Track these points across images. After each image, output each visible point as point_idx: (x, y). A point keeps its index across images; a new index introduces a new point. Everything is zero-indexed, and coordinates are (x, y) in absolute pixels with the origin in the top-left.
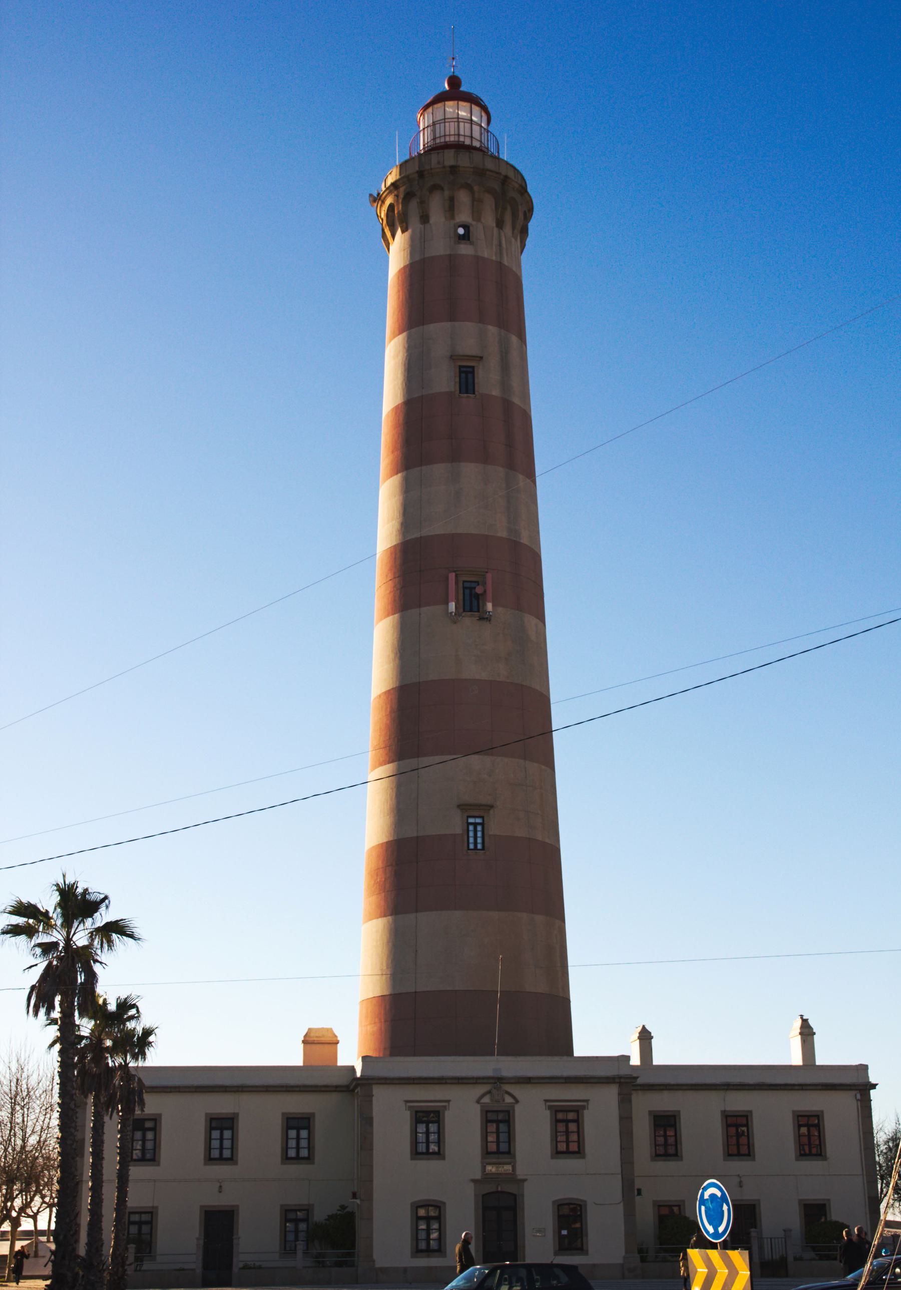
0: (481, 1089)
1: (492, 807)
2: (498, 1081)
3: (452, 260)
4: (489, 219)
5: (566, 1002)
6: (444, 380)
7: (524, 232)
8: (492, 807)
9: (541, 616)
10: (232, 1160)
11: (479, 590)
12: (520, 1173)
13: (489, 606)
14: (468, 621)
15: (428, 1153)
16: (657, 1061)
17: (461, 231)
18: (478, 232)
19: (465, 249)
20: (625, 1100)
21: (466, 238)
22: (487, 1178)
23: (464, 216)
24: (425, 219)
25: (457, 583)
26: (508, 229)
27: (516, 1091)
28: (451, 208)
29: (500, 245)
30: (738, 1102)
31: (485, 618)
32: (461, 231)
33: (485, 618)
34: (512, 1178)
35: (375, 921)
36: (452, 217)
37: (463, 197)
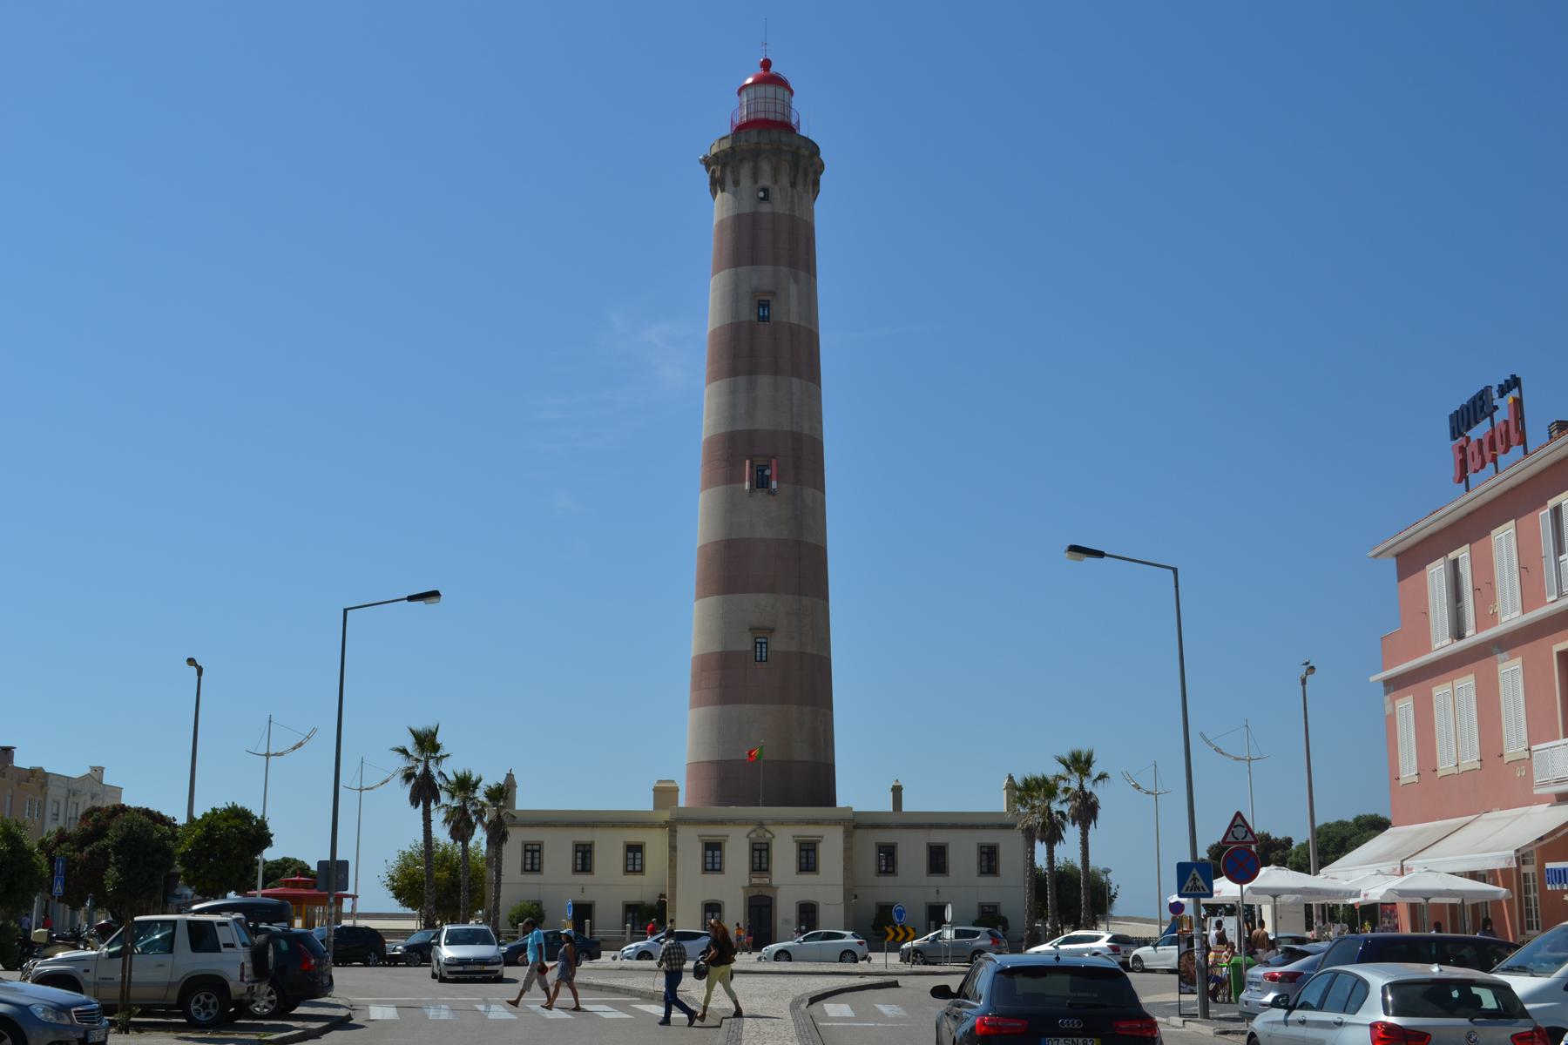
0: (750, 828)
1: (772, 630)
2: (761, 824)
3: (755, 217)
4: (785, 181)
5: (833, 767)
6: (747, 313)
7: (816, 183)
8: (772, 630)
9: (820, 487)
10: (539, 871)
11: (767, 472)
12: (774, 883)
13: (774, 485)
14: (760, 494)
15: (713, 870)
16: (905, 808)
17: (762, 194)
18: (776, 194)
19: (765, 208)
20: (848, 836)
21: (766, 199)
22: (752, 886)
23: (765, 181)
24: (736, 183)
25: (751, 466)
26: (800, 188)
27: (770, 828)
28: (755, 177)
29: (792, 201)
30: (938, 837)
31: (772, 493)
32: (762, 194)
33: (772, 493)
34: (769, 886)
35: (709, 708)
36: (756, 181)
37: (766, 167)
